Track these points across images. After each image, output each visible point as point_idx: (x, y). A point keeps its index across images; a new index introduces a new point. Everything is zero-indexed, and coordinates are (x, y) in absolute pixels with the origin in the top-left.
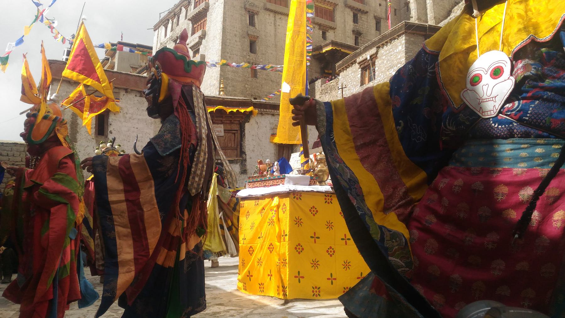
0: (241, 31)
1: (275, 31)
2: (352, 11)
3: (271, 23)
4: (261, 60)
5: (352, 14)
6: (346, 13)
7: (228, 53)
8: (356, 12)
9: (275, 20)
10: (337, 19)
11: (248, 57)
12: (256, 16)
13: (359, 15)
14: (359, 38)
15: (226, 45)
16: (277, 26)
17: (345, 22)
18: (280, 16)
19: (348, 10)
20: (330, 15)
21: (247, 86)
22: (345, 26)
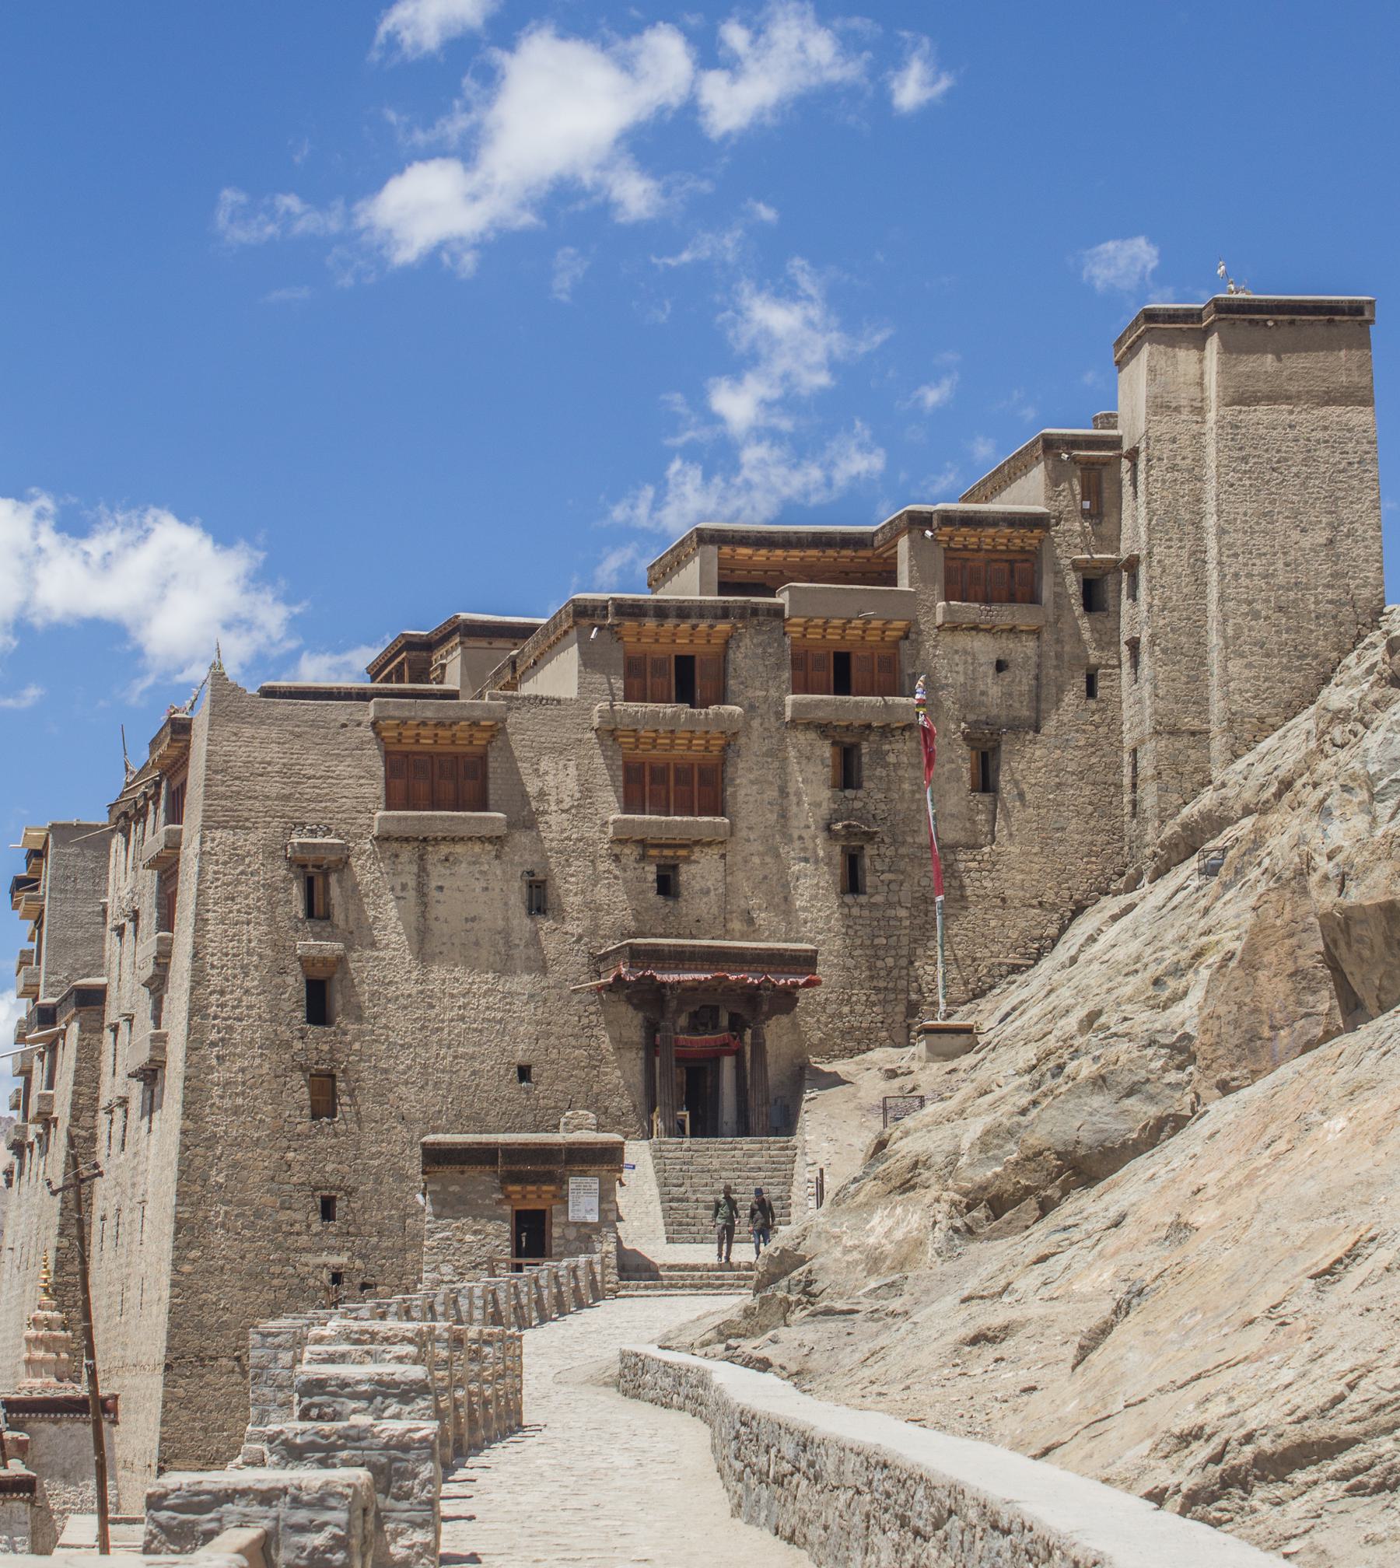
0: (269, 952)
1: (423, 914)
2: (826, 737)
3: (404, 887)
4: (357, 1046)
5: (826, 750)
6: (792, 753)
7: (213, 1044)
8: (848, 740)
9: (423, 871)
10: (741, 797)
11: (298, 1045)
12: (333, 879)
13: (865, 748)
14: (870, 850)
15: (205, 1017)
16: (435, 894)
17: (783, 792)
18: (444, 849)
19: (804, 738)
20: (701, 785)
21: (291, 1155)
22: (783, 815)
